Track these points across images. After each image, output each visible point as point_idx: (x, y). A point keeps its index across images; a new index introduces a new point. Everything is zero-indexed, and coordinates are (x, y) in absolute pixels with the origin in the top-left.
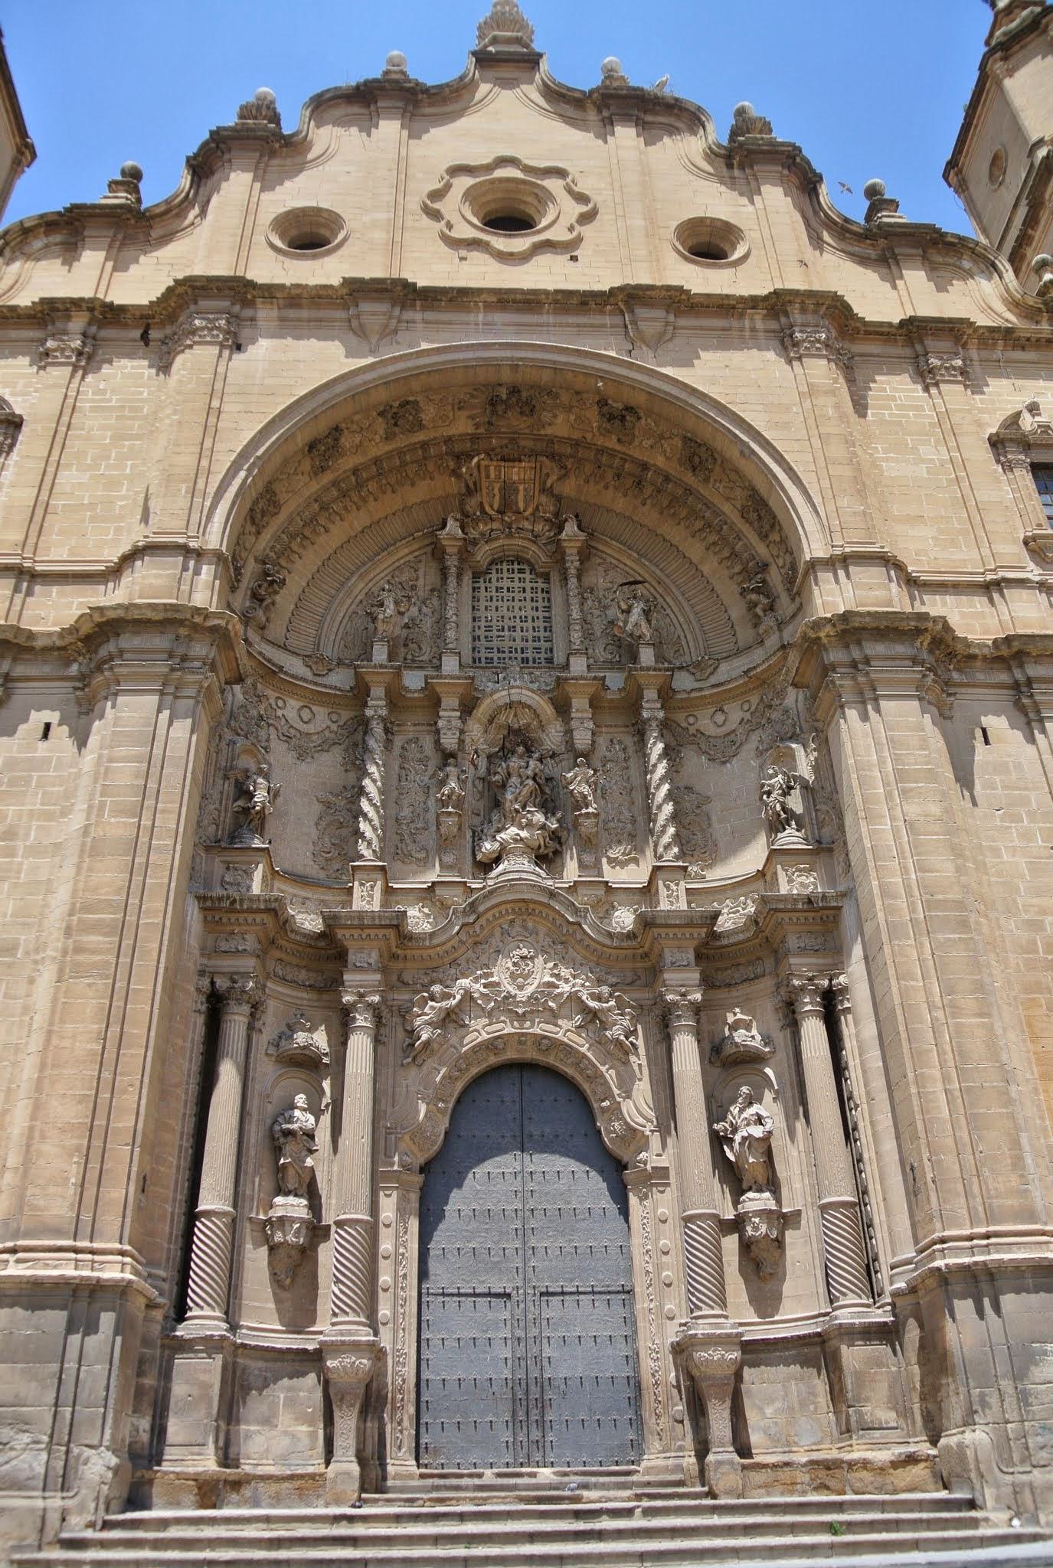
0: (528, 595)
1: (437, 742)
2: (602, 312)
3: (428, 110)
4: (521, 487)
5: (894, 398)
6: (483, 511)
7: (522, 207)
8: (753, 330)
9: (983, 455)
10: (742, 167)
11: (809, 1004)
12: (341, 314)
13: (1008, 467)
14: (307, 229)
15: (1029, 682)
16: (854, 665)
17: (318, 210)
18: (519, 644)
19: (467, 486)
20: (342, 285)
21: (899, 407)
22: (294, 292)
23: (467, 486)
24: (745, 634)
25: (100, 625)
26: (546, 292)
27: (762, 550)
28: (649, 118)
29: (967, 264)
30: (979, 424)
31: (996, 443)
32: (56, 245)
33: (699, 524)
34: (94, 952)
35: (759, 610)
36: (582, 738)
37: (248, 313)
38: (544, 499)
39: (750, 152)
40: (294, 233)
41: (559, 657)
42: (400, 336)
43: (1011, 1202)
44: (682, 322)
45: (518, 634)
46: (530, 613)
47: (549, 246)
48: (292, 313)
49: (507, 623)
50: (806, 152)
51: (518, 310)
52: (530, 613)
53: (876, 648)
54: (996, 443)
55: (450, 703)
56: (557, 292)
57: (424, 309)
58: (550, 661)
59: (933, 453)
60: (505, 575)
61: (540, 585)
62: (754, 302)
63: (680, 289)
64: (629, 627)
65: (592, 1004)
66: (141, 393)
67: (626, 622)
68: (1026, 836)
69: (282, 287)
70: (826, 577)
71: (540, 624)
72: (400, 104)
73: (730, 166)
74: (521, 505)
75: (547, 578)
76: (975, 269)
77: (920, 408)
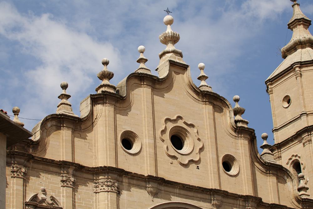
2: (206, 194)
3: (157, 86)
7: (181, 135)
8: (239, 205)
14: (126, 137)
17: (132, 132)
20: (147, 176)
22: (134, 175)
26: (195, 187)
28: (215, 103)
32: (54, 126)
37: (120, 179)
40: (123, 138)
44: (225, 200)
47: (191, 161)
56: (198, 187)
57: (164, 186)
62: (241, 197)
63: (227, 192)
69: (132, 173)
72: (151, 84)
73: (235, 131)
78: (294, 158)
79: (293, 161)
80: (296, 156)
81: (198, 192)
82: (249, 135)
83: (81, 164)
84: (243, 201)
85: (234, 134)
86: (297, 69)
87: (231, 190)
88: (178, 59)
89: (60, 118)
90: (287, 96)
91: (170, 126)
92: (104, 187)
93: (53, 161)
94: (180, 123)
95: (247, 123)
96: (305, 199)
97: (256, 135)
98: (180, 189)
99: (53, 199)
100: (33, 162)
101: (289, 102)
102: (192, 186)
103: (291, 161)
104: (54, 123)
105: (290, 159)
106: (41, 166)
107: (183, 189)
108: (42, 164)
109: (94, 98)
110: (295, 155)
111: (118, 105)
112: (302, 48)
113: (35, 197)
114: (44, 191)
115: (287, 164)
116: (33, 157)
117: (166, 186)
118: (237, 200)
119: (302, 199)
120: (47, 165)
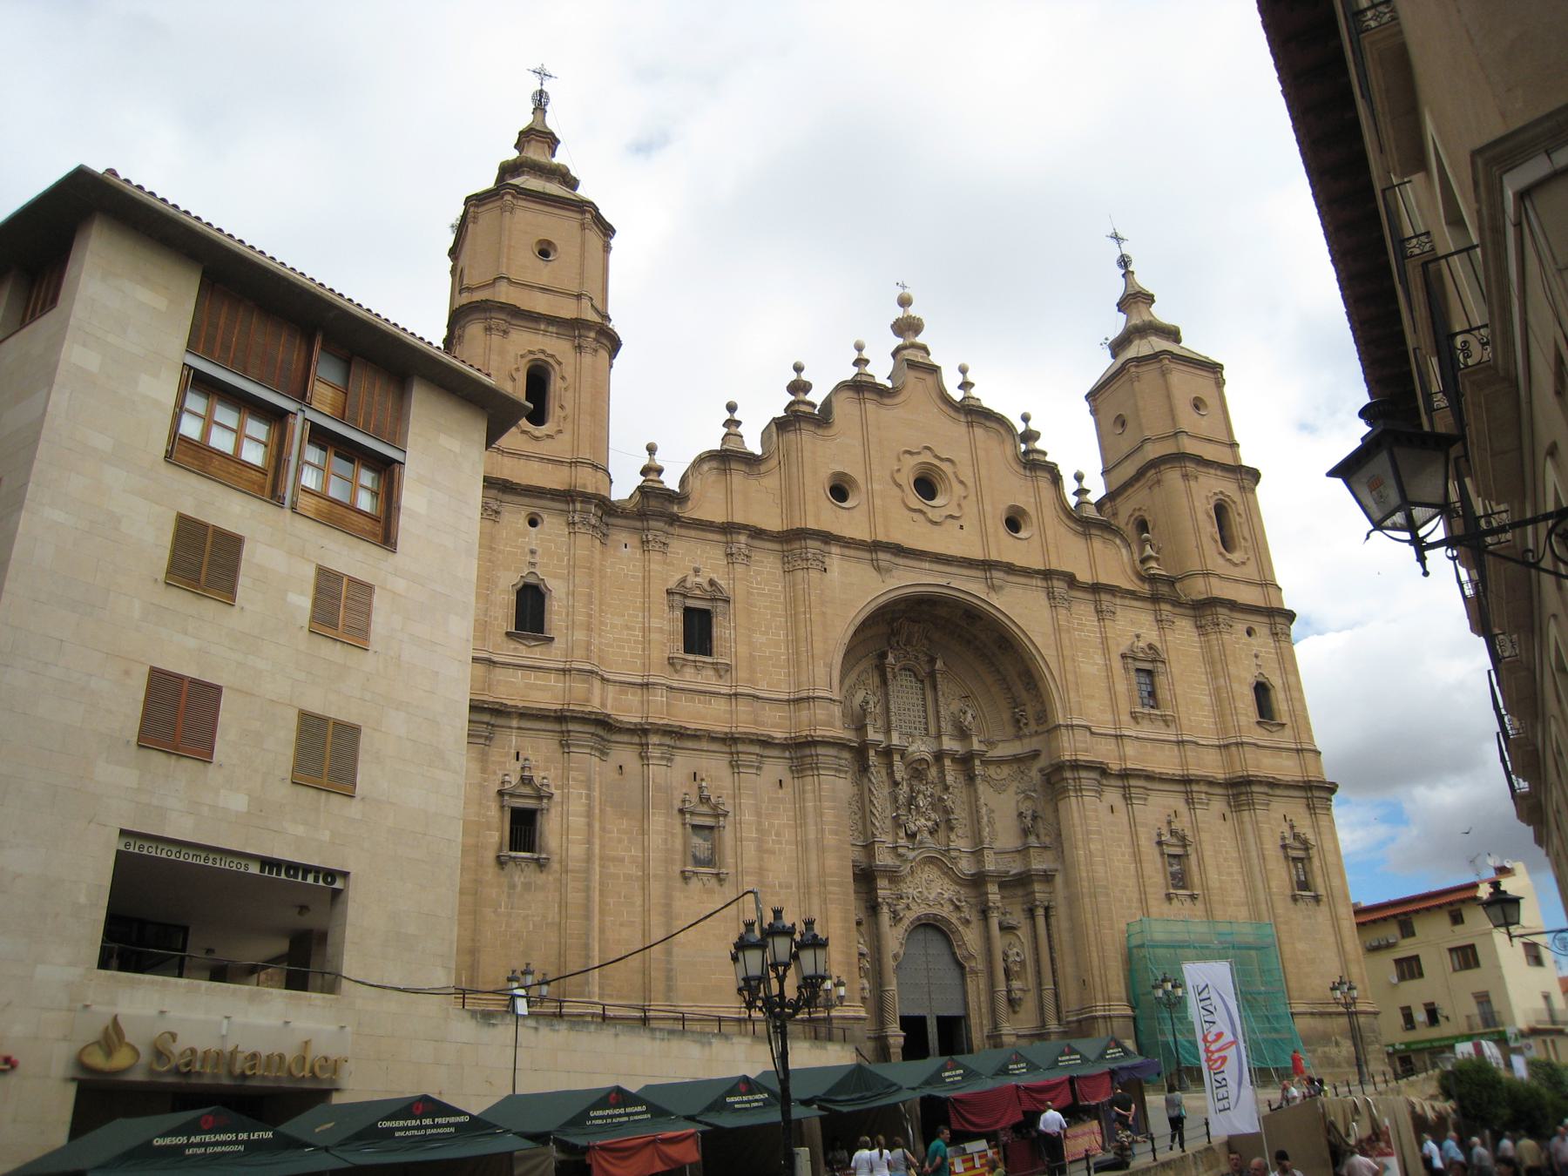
0: (914, 691)
1: (891, 774)
2: (977, 569)
3: (887, 401)
4: (916, 635)
5: (1085, 625)
6: (898, 644)
9: (1117, 664)
10: (1030, 470)
11: (1040, 912)
12: (867, 555)
13: (1126, 669)
15: (1129, 787)
16: (1074, 779)
17: (846, 474)
18: (912, 718)
19: (892, 630)
21: (1088, 631)
23: (892, 630)
24: (1010, 730)
25: (809, 742)
27: (1024, 695)
28: (988, 424)
29: (1118, 541)
30: (1118, 645)
31: (1124, 656)
33: (993, 669)
34: (834, 894)
35: (1022, 725)
36: (949, 779)
38: (925, 642)
39: (1035, 465)
41: (932, 730)
42: (895, 573)
43: (1117, 995)
45: (912, 713)
46: (916, 702)
48: (847, 552)
49: (907, 707)
50: (1059, 468)
51: (944, 564)
52: (916, 702)
53: (1083, 774)
54: (1124, 656)
55: (897, 757)
58: (926, 729)
59: (1099, 660)
60: (904, 677)
61: (919, 685)
62: (1038, 572)
63: (1012, 564)
64: (966, 723)
65: (958, 904)
66: (777, 586)
67: (965, 719)
68: (1123, 855)
70: (1063, 730)
71: (920, 707)
73: (1025, 468)
74: (915, 643)
75: (922, 682)
76: (1121, 546)
77: (1095, 632)
78: (1137, 514)
79: (1136, 519)
80: (1140, 509)
81: (962, 566)
82: (1049, 472)
83: (759, 526)
84: (1043, 579)
85: (1022, 471)
86: (1133, 369)
87: (1019, 561)
88: (922, 357)
89: (723, 456)
90: (1120, 416)
91: (911, 463)
92: (799, 562)
93: (712, 522)
94: (927, 457)
95: (1045, 454)
96: (1154, 574)
97: (1061, 473)
98: (931, 561)
99: (712, 583)
100: (680, 526)
101: (1123, 424)
102: (951, 556)
103: (1132, 519)
104: (714, 464)
105: (1131, 516)
106: (693, 533)
107: (937, 563)
108: (694, 529)
109: (780, 424)
110: (1137, 507)
111: (820, 432)
112: (1142, 338)
113: (684, 580)
114: (697, 571)
115: (1127, 524)
116: (678, 517)
117: (907, 557)
118: (1032, 577)
119: (1150, 575)
120: (703, 530)
